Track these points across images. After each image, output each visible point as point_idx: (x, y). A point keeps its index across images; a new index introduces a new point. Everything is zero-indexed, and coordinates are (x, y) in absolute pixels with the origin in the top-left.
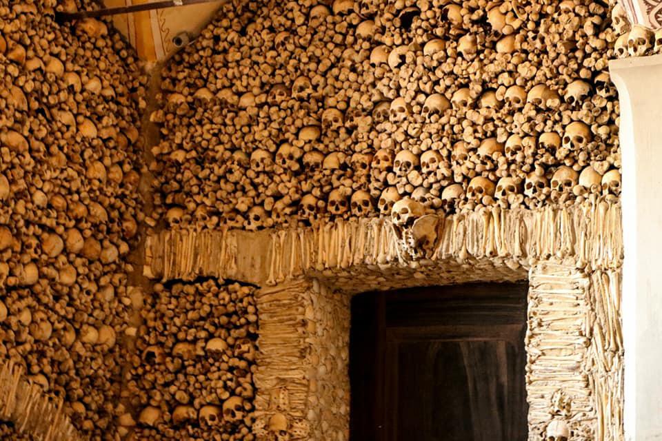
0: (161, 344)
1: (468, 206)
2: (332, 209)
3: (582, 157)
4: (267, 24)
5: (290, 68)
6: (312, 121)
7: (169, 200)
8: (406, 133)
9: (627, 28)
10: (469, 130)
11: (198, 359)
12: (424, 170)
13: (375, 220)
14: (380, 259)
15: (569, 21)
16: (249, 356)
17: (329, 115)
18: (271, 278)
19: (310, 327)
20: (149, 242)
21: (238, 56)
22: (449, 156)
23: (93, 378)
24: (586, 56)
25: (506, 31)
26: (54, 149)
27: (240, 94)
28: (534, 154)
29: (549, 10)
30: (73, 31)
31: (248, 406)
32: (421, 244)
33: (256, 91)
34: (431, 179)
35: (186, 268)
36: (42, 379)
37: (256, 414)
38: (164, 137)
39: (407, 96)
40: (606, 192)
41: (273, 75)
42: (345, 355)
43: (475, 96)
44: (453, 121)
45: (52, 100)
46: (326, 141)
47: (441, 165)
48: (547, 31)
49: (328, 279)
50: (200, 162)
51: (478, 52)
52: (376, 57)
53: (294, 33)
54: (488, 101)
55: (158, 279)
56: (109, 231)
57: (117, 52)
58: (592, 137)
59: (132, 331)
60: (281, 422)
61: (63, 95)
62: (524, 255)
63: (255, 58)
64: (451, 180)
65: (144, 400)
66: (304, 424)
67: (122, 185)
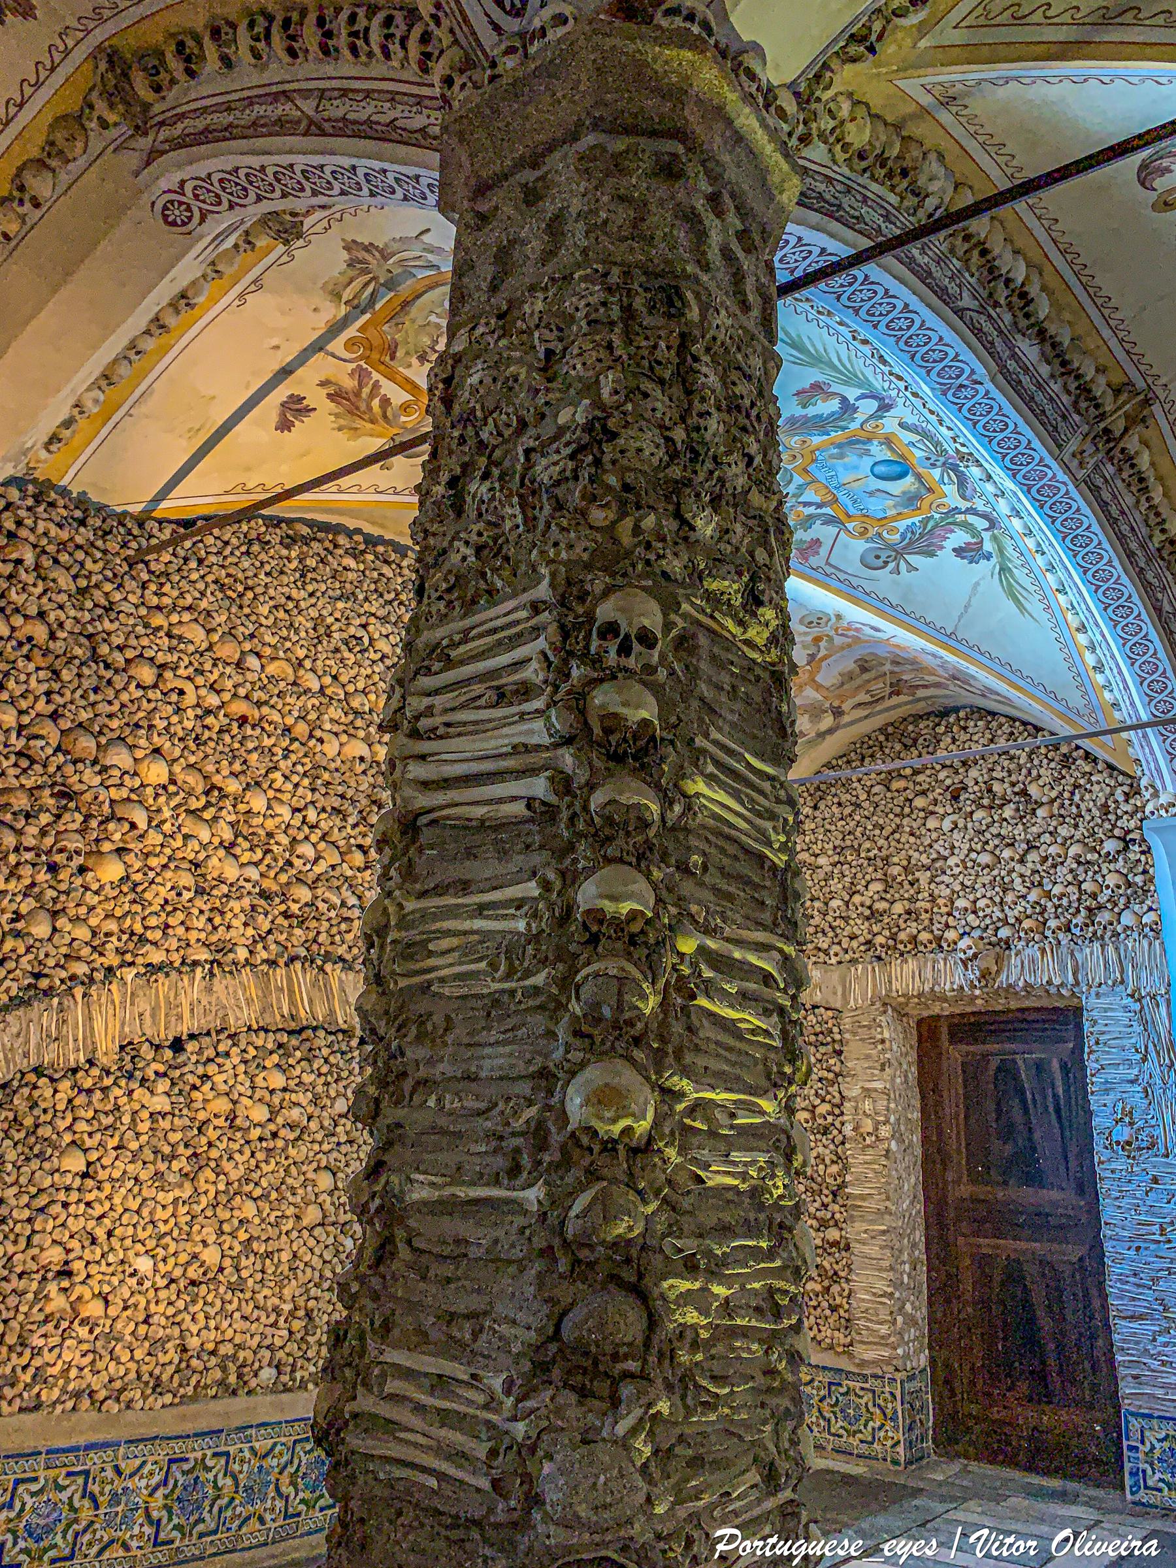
1: (1023, 943)
2: (901, 947)
3: (1122, 901)
4: (836, 800)
5: (858, 834)
6: (879, 875)
8: (962, 884)
9: (1156, 795)
10: (1018, 881)
12: (981, 914)
15: (1101, 790)
16: (837, 1069)
17: (895, 870)
18: (852, 1003)
19: (887, 1044)
21: (813, 826)
24: (1119, 818)
25: (1045, 800)
27: (816, 856)
28: (1079, 900)
29: (1082, 782)
31: (837, 1111)
32: (985, 975)
33: (830, 852)
34: (988, 921)
37: (845, 1118)
40: (1147, 930)
44: (1003, 873)
46: (892, 891)
48: (1082, 799)
51: (1021, 818)
53: (859, 806)
54: (1033, 856)
58: (1129, 885)
60: (868, 1126)
62: (1077, 983)
63: (828, 827)
66: (888, 1127)
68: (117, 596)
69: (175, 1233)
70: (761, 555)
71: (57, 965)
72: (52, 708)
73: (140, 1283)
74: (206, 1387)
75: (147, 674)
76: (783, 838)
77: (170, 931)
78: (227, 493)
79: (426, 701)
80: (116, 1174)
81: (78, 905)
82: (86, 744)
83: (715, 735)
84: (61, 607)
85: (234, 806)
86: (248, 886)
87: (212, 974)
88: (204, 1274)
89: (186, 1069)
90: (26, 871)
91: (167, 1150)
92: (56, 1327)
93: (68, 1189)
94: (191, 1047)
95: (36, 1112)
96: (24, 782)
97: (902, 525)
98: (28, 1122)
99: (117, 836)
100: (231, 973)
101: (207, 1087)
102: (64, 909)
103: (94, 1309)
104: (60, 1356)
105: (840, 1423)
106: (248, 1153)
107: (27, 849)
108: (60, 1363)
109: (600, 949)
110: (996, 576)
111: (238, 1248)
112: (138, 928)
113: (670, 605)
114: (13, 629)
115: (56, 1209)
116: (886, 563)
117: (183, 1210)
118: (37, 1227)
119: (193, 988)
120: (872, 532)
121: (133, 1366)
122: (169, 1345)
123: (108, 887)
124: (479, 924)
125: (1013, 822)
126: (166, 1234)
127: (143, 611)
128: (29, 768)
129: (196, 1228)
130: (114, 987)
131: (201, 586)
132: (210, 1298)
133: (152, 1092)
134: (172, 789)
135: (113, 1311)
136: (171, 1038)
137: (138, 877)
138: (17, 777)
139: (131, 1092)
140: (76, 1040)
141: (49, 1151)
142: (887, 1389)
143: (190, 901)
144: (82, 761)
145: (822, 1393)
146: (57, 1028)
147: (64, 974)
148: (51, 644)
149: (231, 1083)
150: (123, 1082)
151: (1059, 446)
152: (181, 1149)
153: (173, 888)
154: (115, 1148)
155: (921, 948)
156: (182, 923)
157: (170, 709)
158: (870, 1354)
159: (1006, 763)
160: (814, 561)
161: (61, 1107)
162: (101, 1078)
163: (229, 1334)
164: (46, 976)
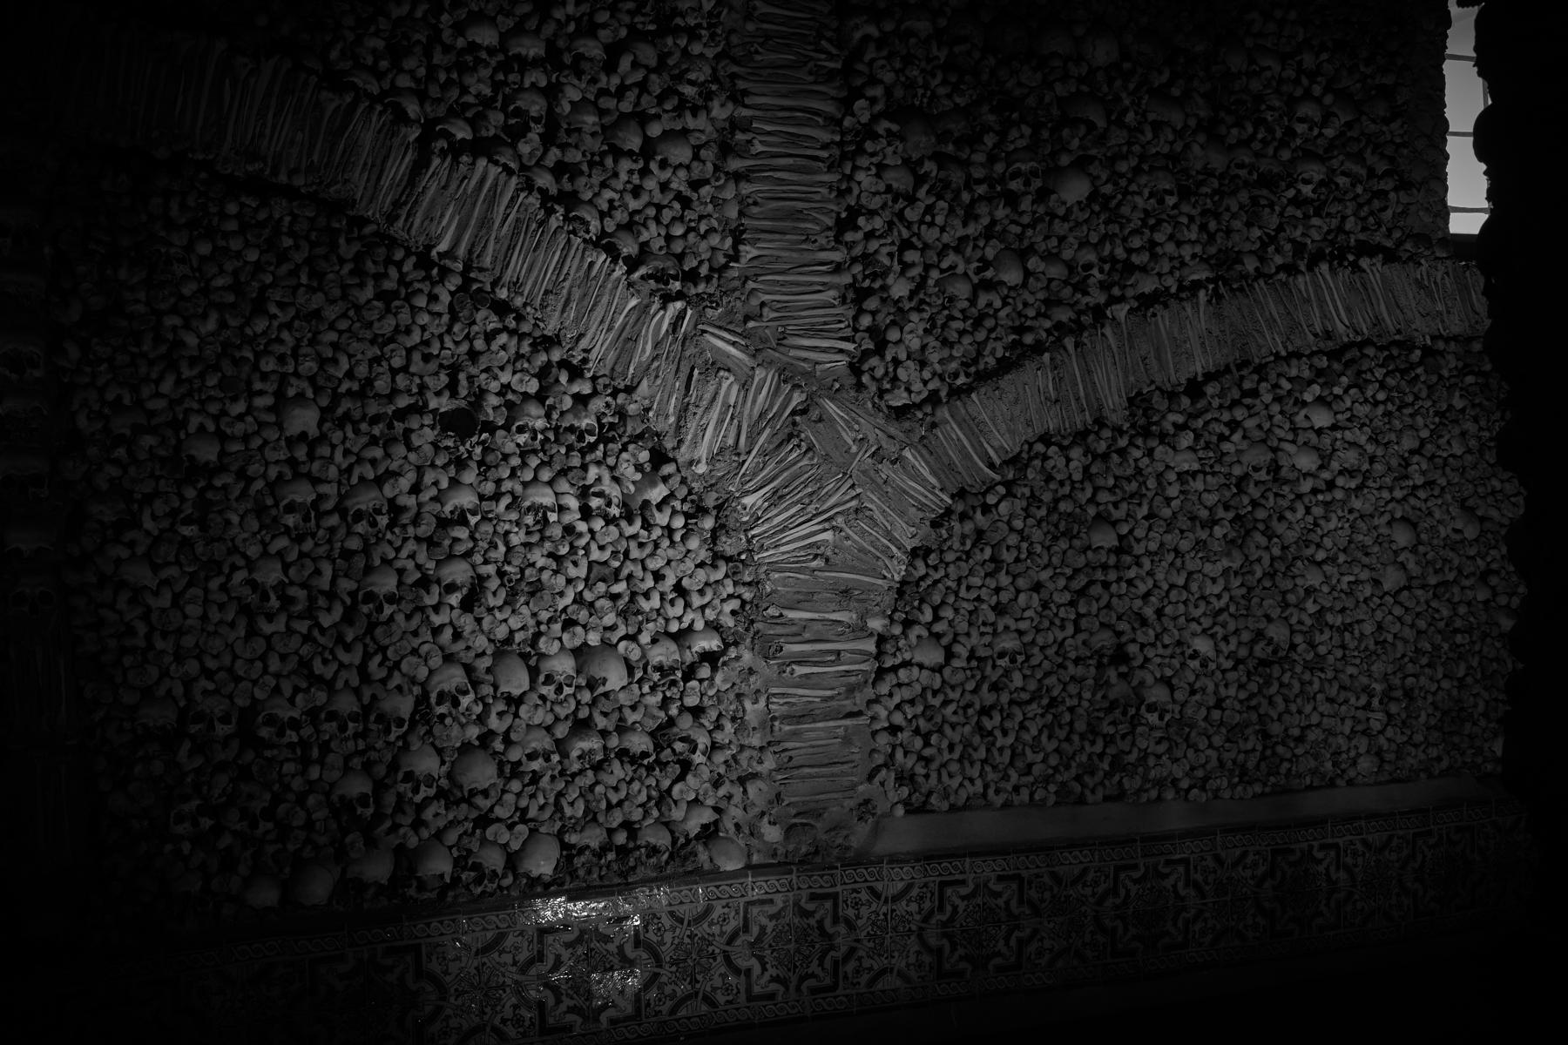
69: (1232, 609)
71: (1039, 314)
73: (1204, 665)
74: (1299, 776)
77: (1159, 250)
80: (1153, 546)
81: (1047, 238)
86: (1243, 173)
87: (1219, 297)
88: (1275, 652)
89: (1209, 416)
90: (982, 209)
91: (1204, 514)
92: (1124, 713)
94: (1210, 389)
95: (1053, 486)
96: (958, 100)
99: (1076, 143)
100: (1241, 289)
101: (1237, 437)
102: (1032, 245)
103: (1158, 694)
104: (1133, 744)
106: (1301, 512)
107: (979, 182)
108: (1135, 750)
111: (1309, 622)
112: (1120, 253)
115: (1096, 590)
117: (1236, 582)
118: (1082, 610)
119: (1197, 318)
121: (1213, 754)
122: (1249, 731)
123: (1075, 209)
126: (1221, 611)
129: (1255, 600)
130: (1108, 331)
132: (1286, 678)
133: (1174, 448)
134: (1127, 66)
135: (1179, 695)
136: (1183, 381)
137: (1108, 189)
138: (949, 96)
140: (1078, 399)
141: (1076, 527)
143: (1175, 206)
146: (1055, 389)
149: (1267, 426)
150: (1139, 442)
152: (1221, 513)
153: (1151, 195)
154: (1146, 518)
161: (1077, 476)
162: (1114, 439)
163: (1315, 719)
164: (1030, 329)
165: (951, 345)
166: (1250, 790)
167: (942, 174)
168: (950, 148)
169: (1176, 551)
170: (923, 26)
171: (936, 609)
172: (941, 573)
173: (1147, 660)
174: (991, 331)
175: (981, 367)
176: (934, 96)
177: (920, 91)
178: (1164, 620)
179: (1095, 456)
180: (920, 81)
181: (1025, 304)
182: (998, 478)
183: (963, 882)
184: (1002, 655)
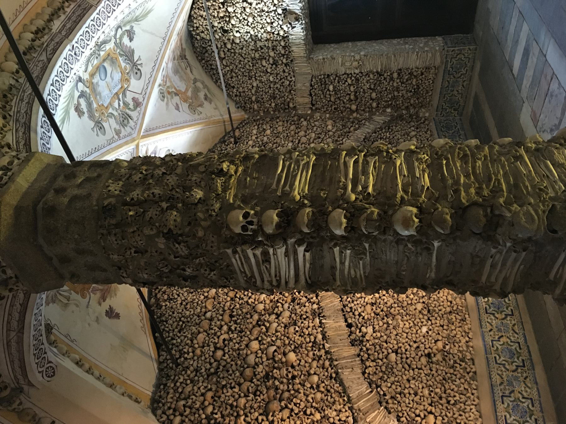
0: (331, 106)
1: (283, 4)
2: (287, 52)
4: (230, 79)
5: (243, 70)
7: (287, 107)
8: (261, 28)
10: (259, 6)
11: (336, 94)
12: (273, 21)
13: (290, 37)
14: (302, 34)
16: (334, 77)
17: (257, 55)
18: (309, 71)
19: (325, 57)
20: (300, 112)
21: (241, 88)
22: (267, 12)
23: (343, 126)
26: (275, 141)
27: (253, 87)
30: (239, 139)
31: (350, 76)
32: (297, 19)
33: (251, 81)
35: (308, 100)
36: (344, 140)
37: (353, 73)
38: (268, 110)
39: (249, 29)
41: (246, 76)
42: (332, 45)
43: (247, 4)
44: (256, 12)
45: (261, 143)
47: (271, 15)
49: (309, 52)
50: (275, 98)
51: (233, 4)
52: (237, 41)
53: (232, 70)
55: (311, 108)
56: (298, 124)
57: (243, 126)
59: (328, 115)
60: (355, 64)
61: (259, 140)
63: (241, 82)
64: (275, 11)
65: (349, 110)
66: (356, 56)
67: (284, 122)
68: (192, 368)
69: (413, 320)
70: (202, 169)
71: (327, 371)
72: (237, 386)
73: (430, 330)
74: (462, 303)
75: (219, 353)
76: (305, 157)
77: (310, 333)
78: (145, 333)
79: (266, 282)
81: (305, 367)
82: (248, 372)
83: (274, 186)
84: (199, 388)
85: (263, 315)
86: (291, 307)
87: (324, 316)
88: (425, 308)
89: (358, 323)
90: (296, 387)
91: (385, 326)
92: (447, 356)
93: (402, 358)
95: (377, 372)
96: (265, 392)
97: (123, 65)
98: (381, 374)
99: (280, 356)
100: (322, 310)
102: (307, 371)
103: (440, 344)
104: (456, 354)
105: (455, 62)
106: (384, 297)
107: (288, 387)
109: (356, 226)
110: (139, 23)
111: (416, 297)
112: (310, 344)
113: (232, 207)
114: (209, 404)
115: (408, 361)
116: (139, 69)
117: (405, 318)
118: (415, 367)
119: (329, 323)
120: (127, 77)
121: (457, 329)
122: (450, 318)
123: (298, 357)
124: (347, 263)
125: (235, 8)
126: (413, 323)
127: (196, 358)
128: (260, 391)
129: (411, 313)
130: (332, 351)
131: (182, 338)
132: (433, 305)
133: (366, 333)
134: (260, 339)
135: (440, 338)
136: (347, 329)
137: (293, 347)
138: (263, 395)
139: (367, 340)
140: (352, 362)
141: (390, 366)
142: (451, 53)
143: (299, 327)
144: (254, 373)
145: (452, 77)
146: (349, 369)
147: (330, 369)
148: (214, 389)
149: (360, 306)
150: (364, 344)
151: (91, 6)
152: (385, 321)
153: (295, 334)
154: (387, 344)
155: (287, 44)
156: (307, 329)
157: (231, 343)
158: (438, 60)
159: (211, 11)
160: (141, 100)
161: (375, 364)
162: (364, 351)
163: (445, 298)
164: (331, 375)
165: (335, 401)
166: (468, 319)
167: (286, 399)
168: (278, 396)
169: (396, 335)
170: (243, 401)
171: (417, 416)
172: (405, 412)
173: (429, 348)
174: (331, 388)
175: (341, 391)
176: (263, 400)
177: (261, 404)
178: (417, 341)
179: (369, 358)
180: (258, 404)
181: (324, 375)
182: (375, 390)
183: (505, 416)
184: (430, 395)
